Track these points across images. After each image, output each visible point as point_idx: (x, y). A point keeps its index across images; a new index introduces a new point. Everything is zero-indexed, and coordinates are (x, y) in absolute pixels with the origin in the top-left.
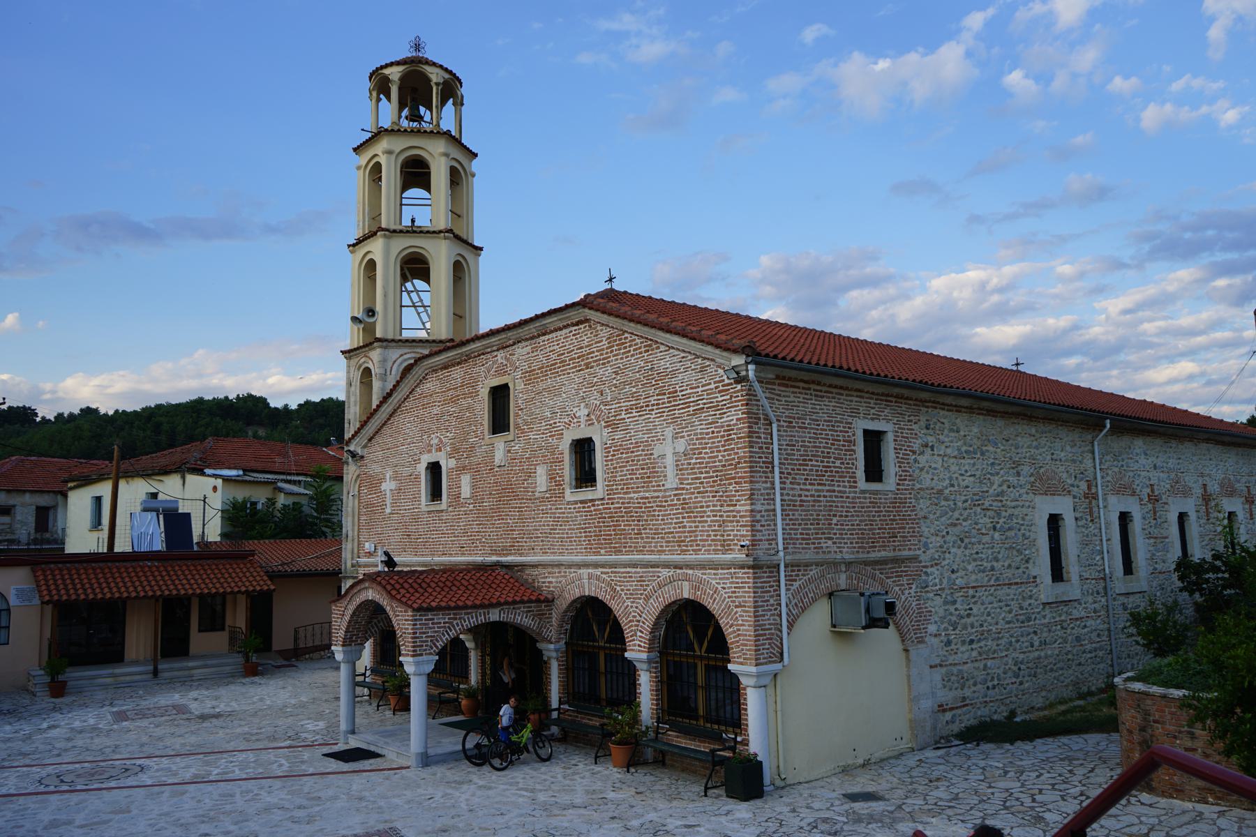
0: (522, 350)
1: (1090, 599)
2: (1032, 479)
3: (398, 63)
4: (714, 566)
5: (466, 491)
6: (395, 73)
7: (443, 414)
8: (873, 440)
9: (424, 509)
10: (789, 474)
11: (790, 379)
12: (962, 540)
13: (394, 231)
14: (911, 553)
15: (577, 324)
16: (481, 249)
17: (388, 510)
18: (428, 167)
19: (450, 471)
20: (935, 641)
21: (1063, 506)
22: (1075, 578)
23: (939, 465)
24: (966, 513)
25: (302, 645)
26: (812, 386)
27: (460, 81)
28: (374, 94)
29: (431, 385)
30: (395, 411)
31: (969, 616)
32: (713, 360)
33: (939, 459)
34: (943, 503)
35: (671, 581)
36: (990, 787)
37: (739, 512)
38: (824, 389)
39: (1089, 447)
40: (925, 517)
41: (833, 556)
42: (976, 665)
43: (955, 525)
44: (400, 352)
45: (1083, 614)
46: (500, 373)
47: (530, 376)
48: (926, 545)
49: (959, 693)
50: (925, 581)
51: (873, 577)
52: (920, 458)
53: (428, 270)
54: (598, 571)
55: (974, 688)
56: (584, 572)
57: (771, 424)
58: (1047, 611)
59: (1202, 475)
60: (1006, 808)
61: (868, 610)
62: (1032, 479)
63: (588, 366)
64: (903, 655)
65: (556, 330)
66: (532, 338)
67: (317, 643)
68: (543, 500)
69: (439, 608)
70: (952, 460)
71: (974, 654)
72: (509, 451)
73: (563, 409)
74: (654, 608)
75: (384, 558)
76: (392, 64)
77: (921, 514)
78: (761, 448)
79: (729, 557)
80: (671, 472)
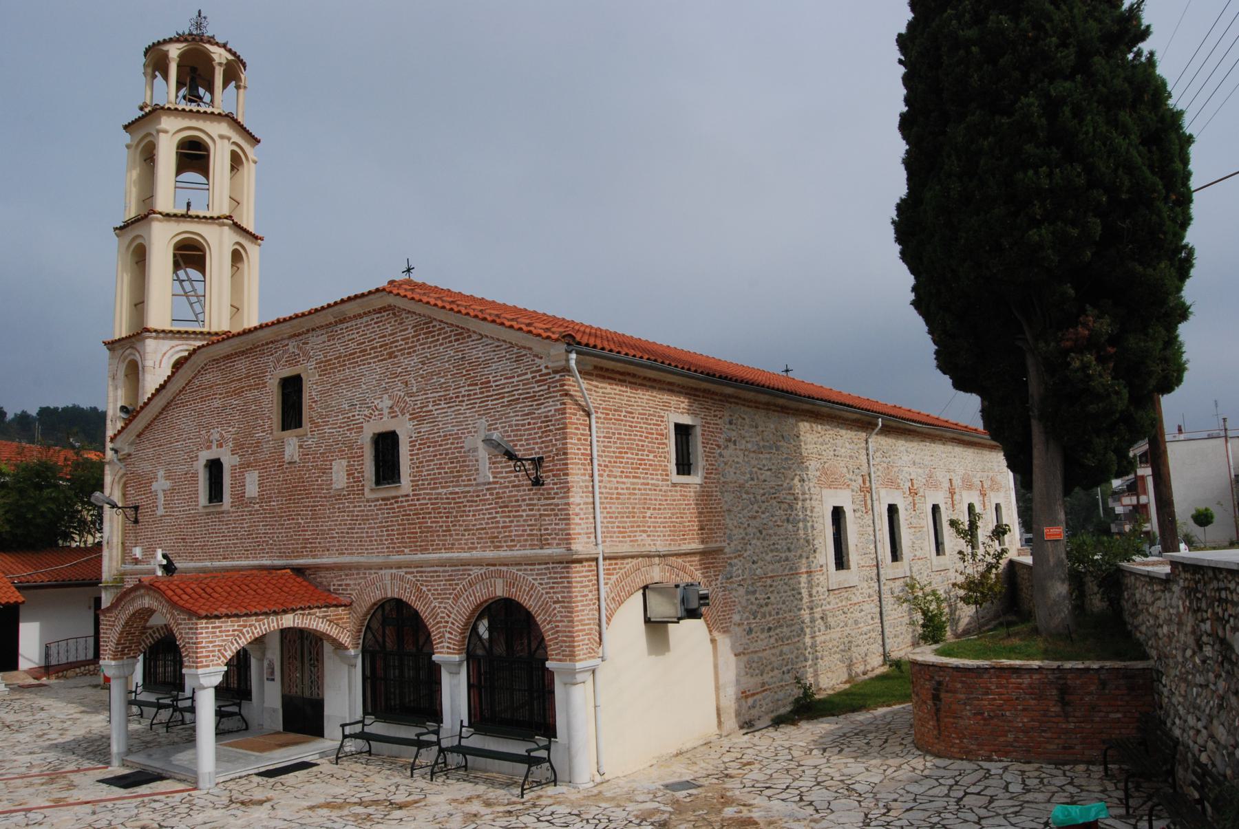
0: (317, 341)
1: (865, 585)
2: (818, 474)
3: (178, 40)
4: (531, 562)
5: (252, 490)
6: (174, 51)
7: (224, 408)
8: (683, 432)
9: (201, 510)
10: (606, 466)
11: (607, 370)
12: (761, 532)
13: (168, 215)
14: (718, 545)
15: (380, 311)
16: (262, 239)
18: (206, 149)
19: (234, 468)
20: (737, 629)
21: (844, 498)
22: (853, 564)
23: (740, 460)
24: (764, 506)
25: (54, 662)
26: (628, 378)
27: (241, 61)
28: (150, 70)
29: (210, 377)
31: (767, 605)
33: (740, 453)
34: (745, 496)
35: (483, 577)
36: (800, 765)
38: (639, 381)
39: (864, 445)
40: (729, 510)
41: (648, 549)
42: (774, 651)
43: (755, 518)
45: (861, 599)
47: (325, 367)
48: (730, 538)
49: (759, 679)
50: (730, 572)
51: (684, 569)
52: (725, 452)
53: (203, 258)
54: (402, 572)
55: (771, 674)
56: (387, 573)
57: (589, 415)
58: (832, 597)
59: (949, 471)
60: (818, 784)
61: (683, 601)
62: (818, 474)
63: (391, 355)
64: (710, 646)
67: (72, 659)
68: (338, 496)
69: (228, 616)
70: (752, 455)
71: (772, 640)
73: (363, 402)
74: (466, 605)
75: (165, 562)
76: (171, 41)
77: (725, 508)
78: (579, 439)
79: (547, 551)
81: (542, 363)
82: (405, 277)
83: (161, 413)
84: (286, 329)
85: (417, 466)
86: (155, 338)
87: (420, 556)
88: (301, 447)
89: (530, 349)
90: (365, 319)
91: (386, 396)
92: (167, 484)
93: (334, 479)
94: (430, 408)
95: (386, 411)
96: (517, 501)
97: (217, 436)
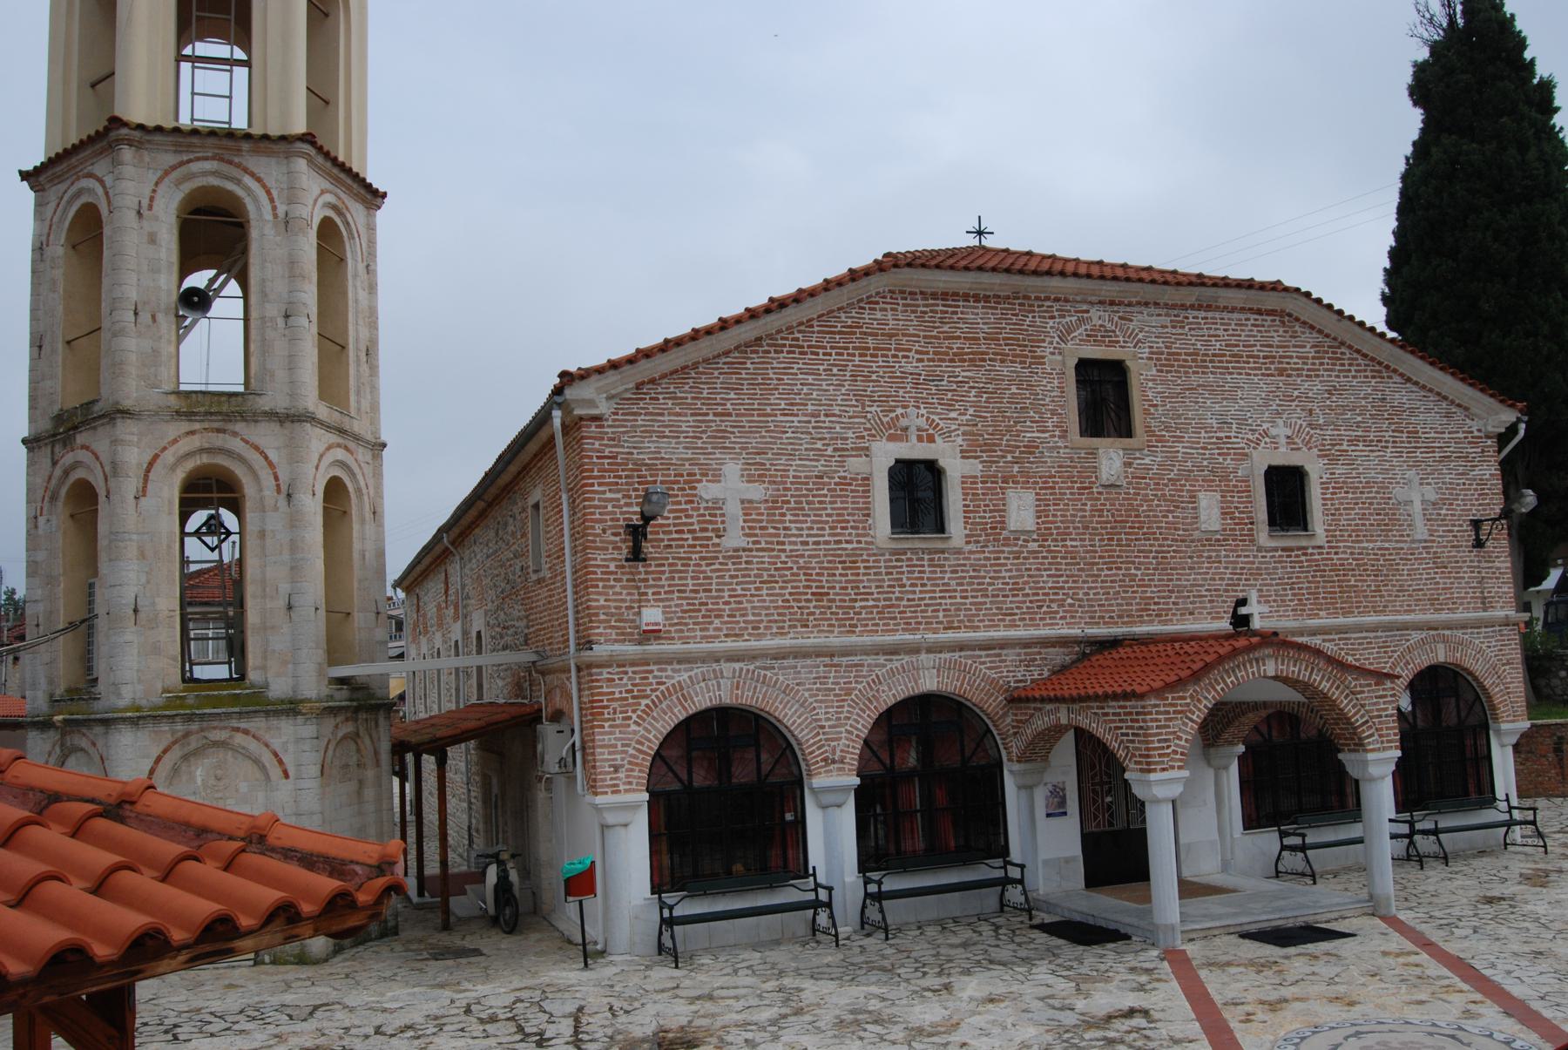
4: (1477, 625)
30: (760, 339)
44: (326, 185)
46: (1091, 337)
47: (1166, 361)
63: (1281, 372)
66: (1174, 307)
68: (1209, 540)
72: (1130, 464)
73: (1242, 422)
81: (1475, 426)
82: (972, 241)
83: (727, 353)
84: (1110, 289)
85: (1332, 514)
86: (311, 162)
87: (1341, 620)
88: (1128, 464)
89: (1466, 409)
90: (1235, 316)
92: (757, 492)
93: (1203, 518)
95: (1283, 440)
97: (922, 422)
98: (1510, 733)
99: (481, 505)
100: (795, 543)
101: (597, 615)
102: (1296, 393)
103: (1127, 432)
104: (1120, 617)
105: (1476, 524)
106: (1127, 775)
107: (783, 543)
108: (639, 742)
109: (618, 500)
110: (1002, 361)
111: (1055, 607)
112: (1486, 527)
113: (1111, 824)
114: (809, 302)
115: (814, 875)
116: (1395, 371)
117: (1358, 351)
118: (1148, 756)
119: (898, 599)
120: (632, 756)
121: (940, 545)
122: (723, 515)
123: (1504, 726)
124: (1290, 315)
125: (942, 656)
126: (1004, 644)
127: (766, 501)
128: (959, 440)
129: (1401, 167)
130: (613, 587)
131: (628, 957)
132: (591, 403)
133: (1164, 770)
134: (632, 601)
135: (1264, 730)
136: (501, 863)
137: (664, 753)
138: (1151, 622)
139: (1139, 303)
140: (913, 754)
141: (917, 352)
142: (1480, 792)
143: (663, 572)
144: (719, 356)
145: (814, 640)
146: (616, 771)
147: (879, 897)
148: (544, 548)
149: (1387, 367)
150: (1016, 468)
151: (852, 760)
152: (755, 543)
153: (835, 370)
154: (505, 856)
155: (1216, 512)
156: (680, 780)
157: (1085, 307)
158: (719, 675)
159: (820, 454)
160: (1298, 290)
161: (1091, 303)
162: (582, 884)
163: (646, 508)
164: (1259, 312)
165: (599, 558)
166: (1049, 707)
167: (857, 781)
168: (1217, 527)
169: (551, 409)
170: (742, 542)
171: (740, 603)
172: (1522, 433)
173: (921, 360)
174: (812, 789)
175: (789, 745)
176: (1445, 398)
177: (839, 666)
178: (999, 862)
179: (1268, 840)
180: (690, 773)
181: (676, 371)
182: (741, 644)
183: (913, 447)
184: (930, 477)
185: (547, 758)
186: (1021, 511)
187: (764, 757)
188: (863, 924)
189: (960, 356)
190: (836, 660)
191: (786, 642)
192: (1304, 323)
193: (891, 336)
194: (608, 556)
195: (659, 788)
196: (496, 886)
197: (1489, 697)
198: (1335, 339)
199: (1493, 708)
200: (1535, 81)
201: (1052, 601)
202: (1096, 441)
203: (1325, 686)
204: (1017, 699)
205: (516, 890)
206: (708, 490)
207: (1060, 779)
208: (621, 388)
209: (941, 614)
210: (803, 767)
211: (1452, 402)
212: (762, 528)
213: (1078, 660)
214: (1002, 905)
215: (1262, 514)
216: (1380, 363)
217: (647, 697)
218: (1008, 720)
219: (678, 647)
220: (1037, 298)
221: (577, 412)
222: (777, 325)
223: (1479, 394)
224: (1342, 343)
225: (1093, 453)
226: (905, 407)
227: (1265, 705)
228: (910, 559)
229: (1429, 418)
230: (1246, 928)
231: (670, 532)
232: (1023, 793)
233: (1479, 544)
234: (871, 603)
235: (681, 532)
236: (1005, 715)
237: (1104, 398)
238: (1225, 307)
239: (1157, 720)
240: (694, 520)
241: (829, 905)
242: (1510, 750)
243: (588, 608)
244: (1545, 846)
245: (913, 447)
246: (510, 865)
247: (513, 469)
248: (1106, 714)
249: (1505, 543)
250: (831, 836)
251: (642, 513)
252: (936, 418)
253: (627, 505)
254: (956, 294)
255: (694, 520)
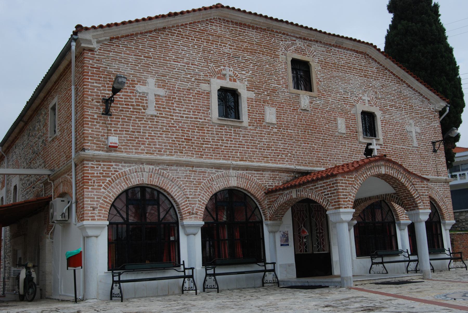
4: (436, 181)
17: (151, 111)
19: (250, 100)
30: (164, 28)
32: (429, 100)
37: (442, 161)
46: (296, 50)
47: (324, 65)
63: (365, 76)
65: (345, 48)
66: (327, 44)
68: (341, 136)
73: (352, 93)
79: (439, 177)
80: (415, 140)
81: (432, 107)
83: (151, 32)
85: (385, 132)
88: (311, 103)
89: (429, 100)
90: (349, 52)
91: (366, 95)
92: (162, 92)
93: (339, 127)
94: (388, 108)
95: (367, 102)
96: (428, 157)
97: (231, 73)
98: (449, 224)
99: (22, 124)
100: (178, 116)
101: (88, 137)
102: (371, 85)
103: (311, 90)
104: (309, 163)
105: (434, 143)
106: (327, 213)
107: (173, 116)
108: (105, 197)
109: (100, 87)
110: (263, 54)
111: (284, 156)
112: (437, 145)
113: (306, 251)
114: (186, 15)
115: (184, 264)
116: (404, 82)
117: (392, 73)
118: (339, 201)
119: (221, 145)
120: (101, 203)
121: (238, 124)
122: (147, 100)
123: (447, 222)
124: (368, 55)
125: (239, 172)
126: (264, 169)
127: (166, 97)
128: (246, 83)
129: (385, 33)
130: (95, 125)
131: (95, 300)
132: (90, 42)
133: (345, 208)
134: (104, 133)
135: (363, 217)
136: (28, 268)
137: (115, 204)
138: (321, 167)
139: (314, 41)
140: (225, 217)
141: (229, 45)
142: (439, 247)
143: (119, 122)
144: (147, 32)
145: (184, 158)
146: (94, 210)
147: (214, 275)
148: (57, 122)
149: (402, 80)
150: (268, 98)
151: (201, 212)
152: (160, 114)
153: (196, 47)
154: (30, 265)
155: (344, 126)
156: (122, 217)
157: (294, 39)
158: (143, 171)
159: (189, 80)
160: (372, 44)
161: (297, 37)
162: (75, 261)
163: (115, 86)
164: (357, 52)
165: (90, 112)
166: (286, 192)
167: (203, 223)
168: (344, 132)
169: (71, 42)
170: (155, 113)
171: (153, 139)
172: (448, 111)
173: (231, 49)
174: (183, 226)
175: (173, 206)
176: (421, 95)
177: (196, 171)
178: (263, 264)
179: (366, 261)
180: (127, 214)
181: (128, 36)
182: (152, 157)
183: (227, 83)
184: (233, 98)
185: (55, 214)
186: (271, 115)
187: (161, 210)
188: (204, 288)
189: (246, 50)
190: (194, 169)
191: (174, 158)
192: (373, 59)
193: (219, 37)
194: (93, 110)
195: (112, 221)
196: (25, 280)
197: (441, 210)
198: (384, 67)
199: (442, 214)
200: (433, 4)
201: (283, 154)
202: (299, 91)
203: (403, 180)
204: (269, 192)
205: (35, 280)
206: (140, 88)
207: (286, 230)
208: (103, 38)
209: (238, 154)
210: (179, 216)
211: (424, 97)
212: (163, 108)
213: (293, 179)
214: (263, 283)
215: (360, 129)
216: (399, 78)
217: (110, 177)
218: (266, 202)
219: (124, 155)
220: (276, 32)
221: (83, 45)
222: (173, 22)
223: (433, 94)
224: (386, 69)
225: (298, 96)
226: (225, 66)
227: (370, 198)
228: (226, 129)
229: (416, 101)
230: (377, 281)
231: (123, 104)
232: (271, 234)
233: (435, 151)
234: (209, 146)
235: (128, 105)
236: (264, 200)
237: (302, 74)
238: (345, 48)
239: (342, 186)
240: (134, 100)
241: (192, 276)
242: (448, 231)
243: (83, 134)
244: (466, 267)
245: (227, 83)
246: (32, 270)
247: (42, 95)
248: (317, 188)
249: (443, 152)
250: (191, 248)
251: (113, 87)
252: (237, 72)
253: (103, 90)
254: (245, 25)
255: (134, 100)
